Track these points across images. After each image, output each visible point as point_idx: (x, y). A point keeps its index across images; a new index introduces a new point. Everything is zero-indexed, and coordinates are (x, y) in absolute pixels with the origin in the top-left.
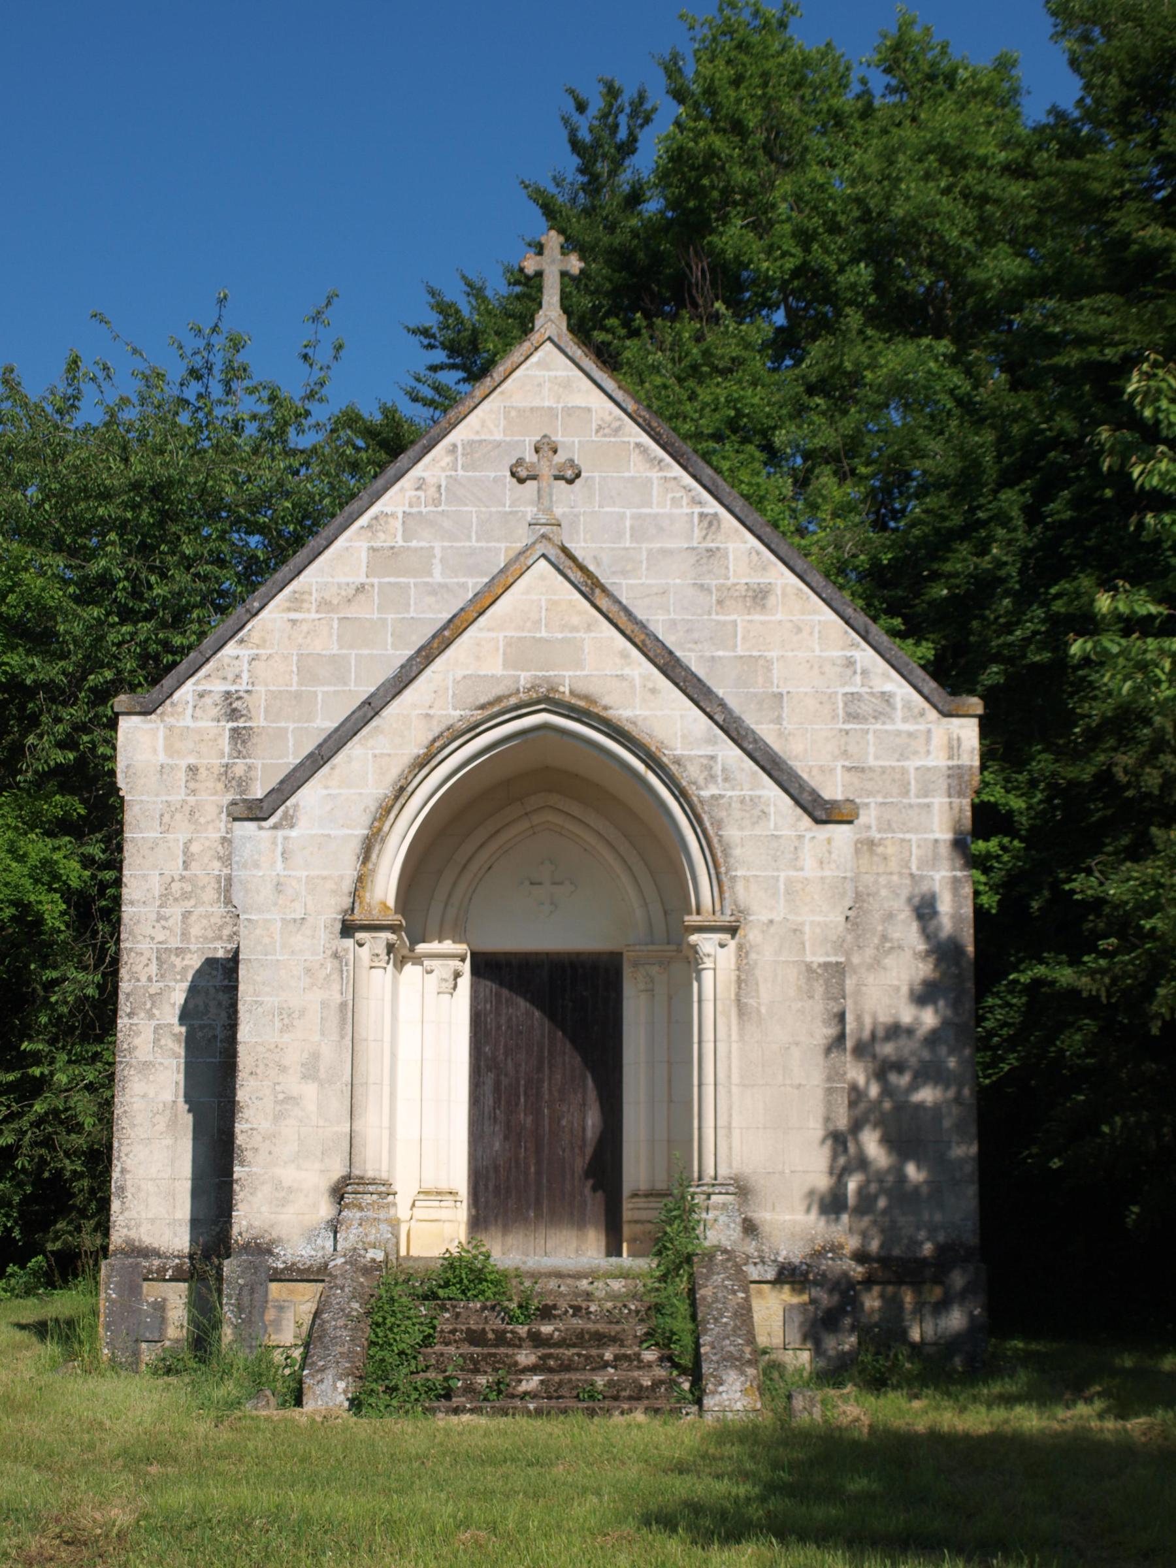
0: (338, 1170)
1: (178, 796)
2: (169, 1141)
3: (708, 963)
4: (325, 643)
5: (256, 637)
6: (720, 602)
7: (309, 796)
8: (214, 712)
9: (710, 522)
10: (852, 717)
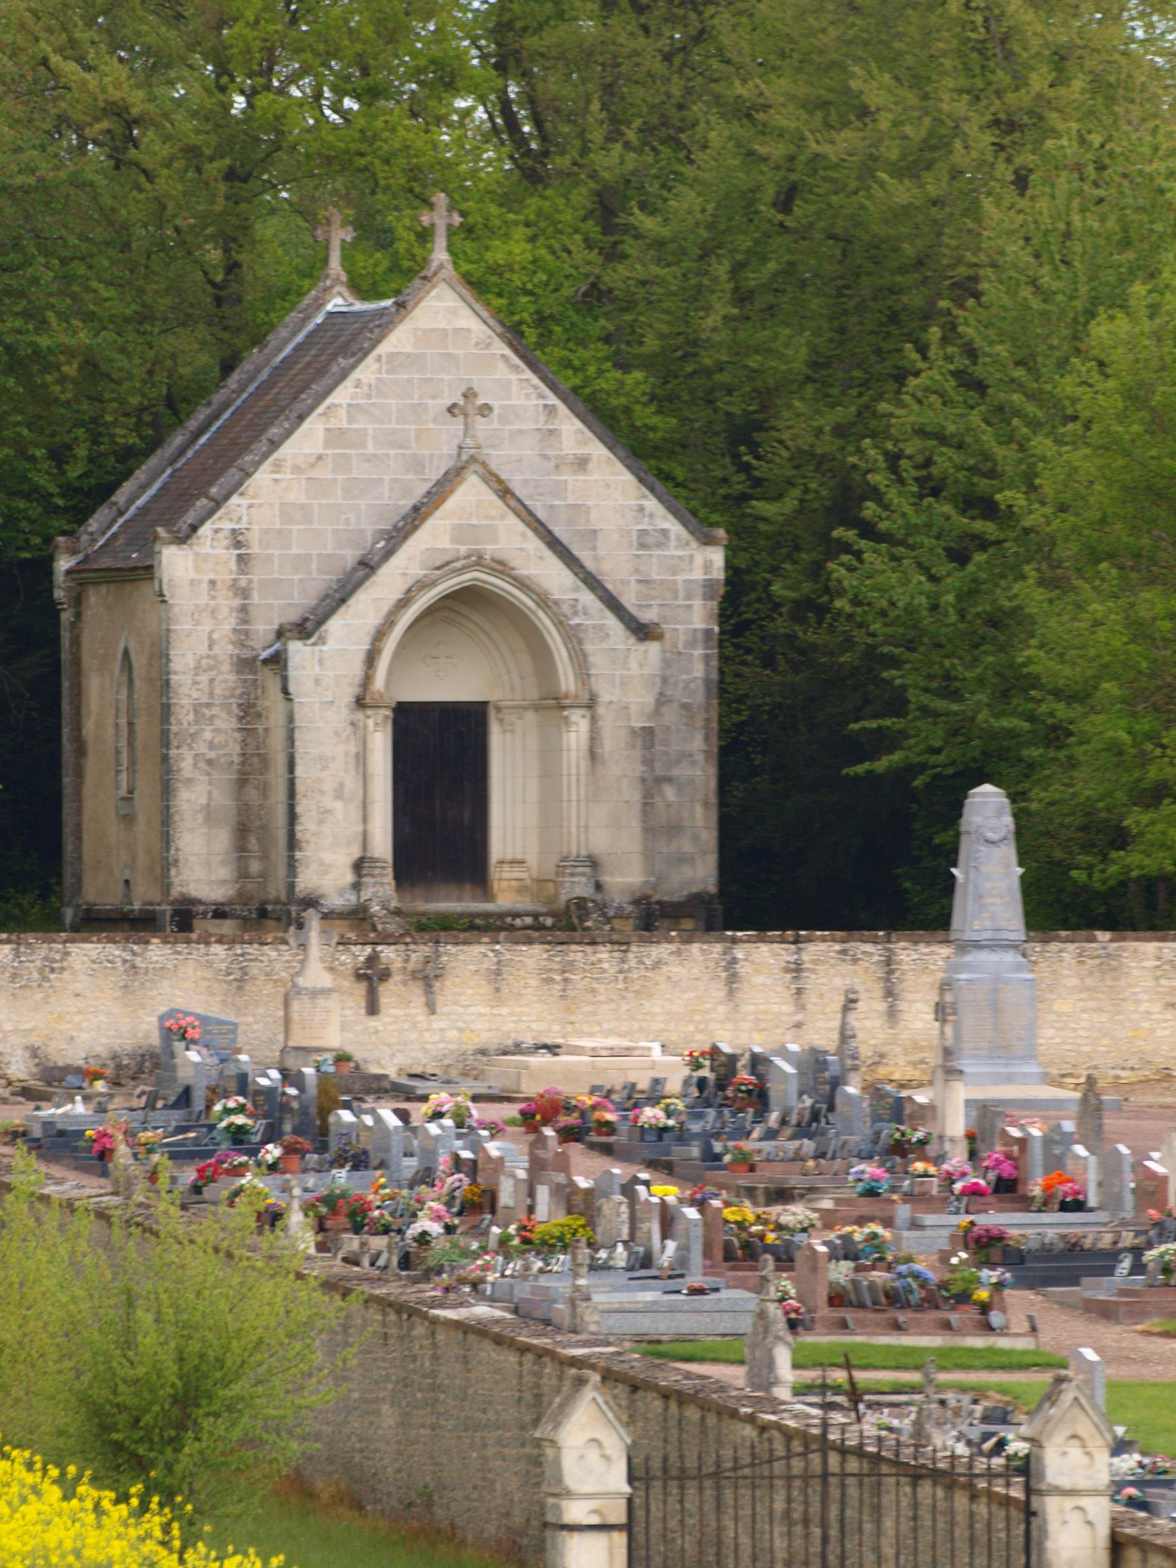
0: (356, 853)
1: (203, 600)
4: (297, 496)
5: (251, 491)
8: (225, 543)
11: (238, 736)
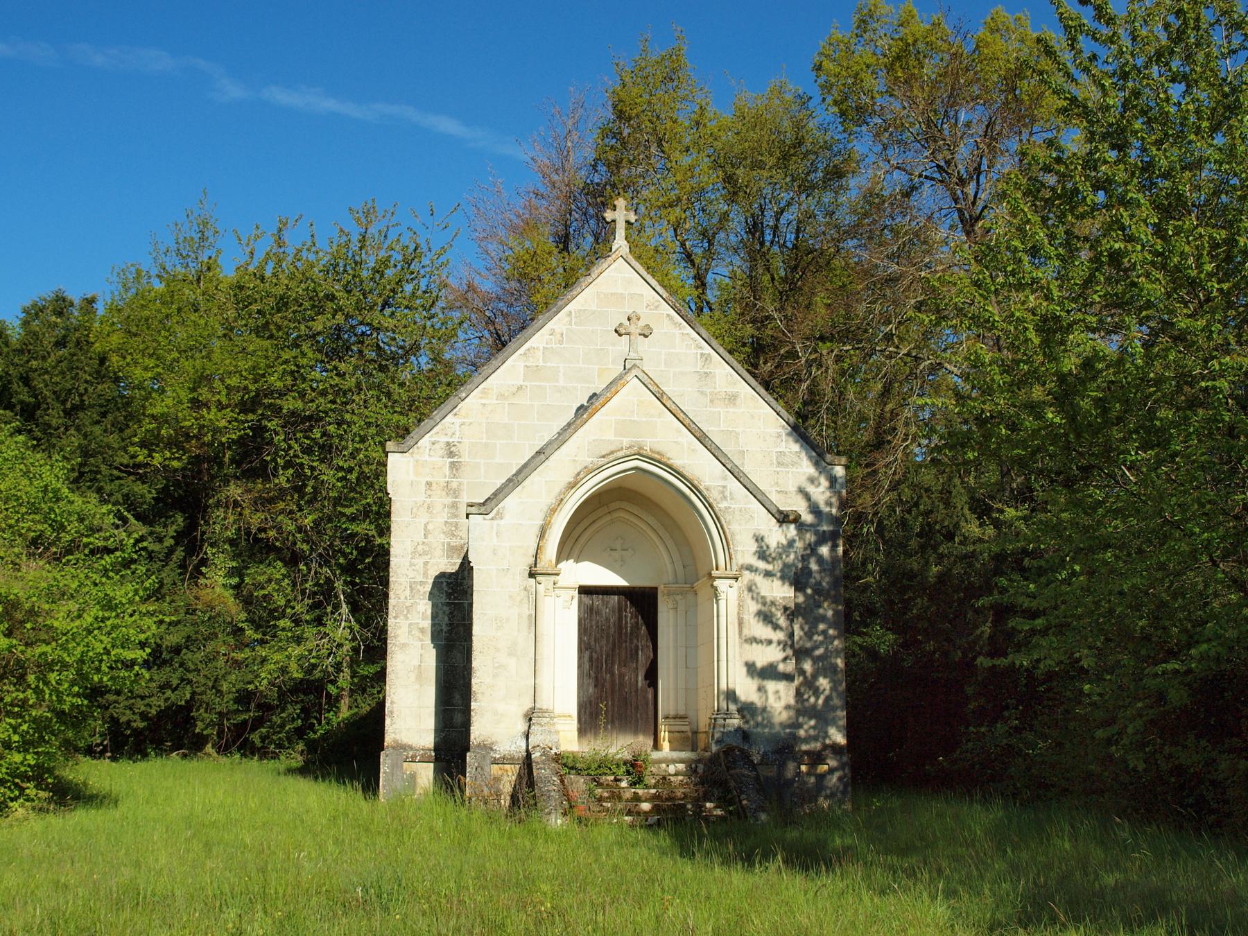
2: (417, 687)
3: (722, 597)
5: (463, 412)
6: (711, 401)
7: (511, 503)
8: (441, 452)
9: (707, 358)
10: (780, 464)
11: (446, 609)
